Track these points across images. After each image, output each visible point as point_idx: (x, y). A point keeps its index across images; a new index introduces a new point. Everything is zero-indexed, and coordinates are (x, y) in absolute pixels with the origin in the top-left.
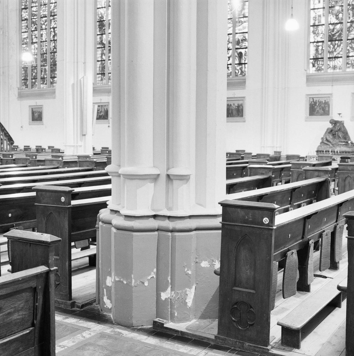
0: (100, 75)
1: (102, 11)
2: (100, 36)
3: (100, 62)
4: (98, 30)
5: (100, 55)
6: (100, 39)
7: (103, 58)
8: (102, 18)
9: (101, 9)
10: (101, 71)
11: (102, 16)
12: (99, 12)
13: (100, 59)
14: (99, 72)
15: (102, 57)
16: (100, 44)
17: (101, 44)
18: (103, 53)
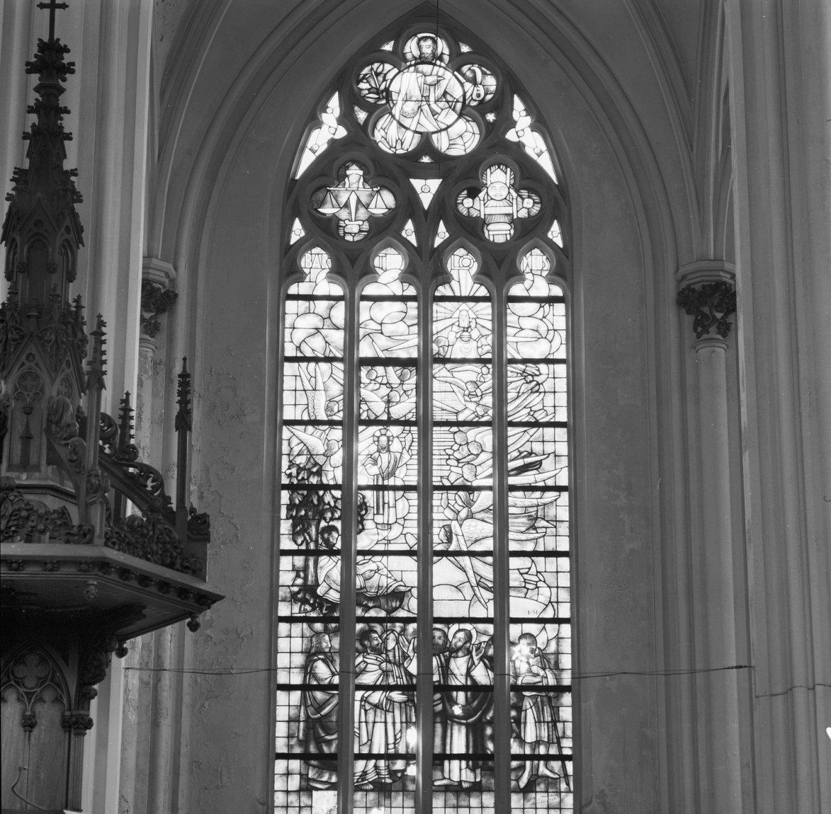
0: (295, 765)
1: (313, 439)
2: (299, 561)
3: (296, 696)
4: (285, 526)
5: (299, 660)
6: (298, 576)
7: (315, 676)
8: (311, 473)
9: (310, 428)
10: (304, 743)
11: (316, 464)
12: (295, 441)
13: (297, 679)
14: (289, 746)
15: (307, 669)
16: (294, 598)
17: (304, 601)
18: (320, 651)
